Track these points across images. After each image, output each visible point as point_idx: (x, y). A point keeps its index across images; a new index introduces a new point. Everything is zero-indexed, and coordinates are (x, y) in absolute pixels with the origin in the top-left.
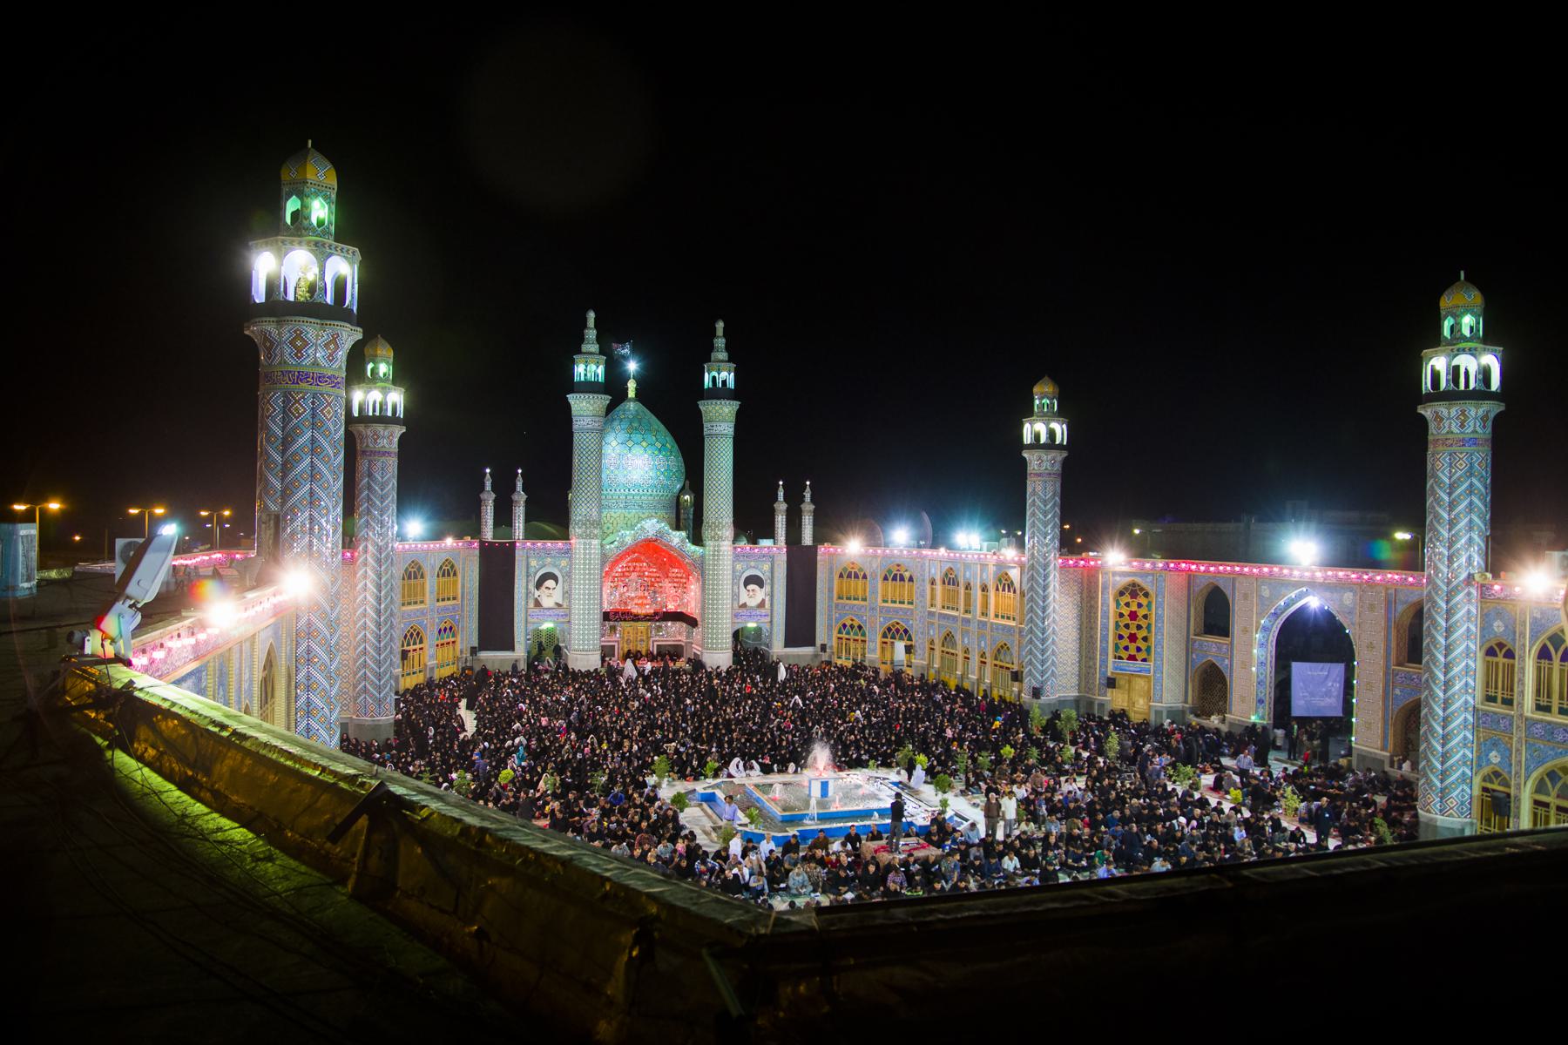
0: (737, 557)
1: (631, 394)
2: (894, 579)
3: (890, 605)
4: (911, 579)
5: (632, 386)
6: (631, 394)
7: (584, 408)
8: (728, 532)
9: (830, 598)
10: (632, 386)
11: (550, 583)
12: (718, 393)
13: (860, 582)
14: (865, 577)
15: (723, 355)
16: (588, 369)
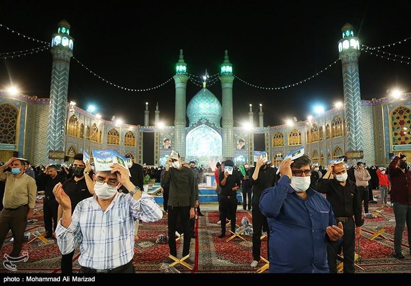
0: (235, 131)
1: (204, 86)
2: (294, 135)
3: (292, 145)
4: (300, 134)
5: (204, 84)
6: (204, 86)
7: (180, 84)
8: (232, 123)
9: (271, 147)
10: (204, 84)
11: (167, 141)
12: (224, 74)
13: (281, 138)
14: (283, 136)
15: (227, 61)
16: (181, 68)
